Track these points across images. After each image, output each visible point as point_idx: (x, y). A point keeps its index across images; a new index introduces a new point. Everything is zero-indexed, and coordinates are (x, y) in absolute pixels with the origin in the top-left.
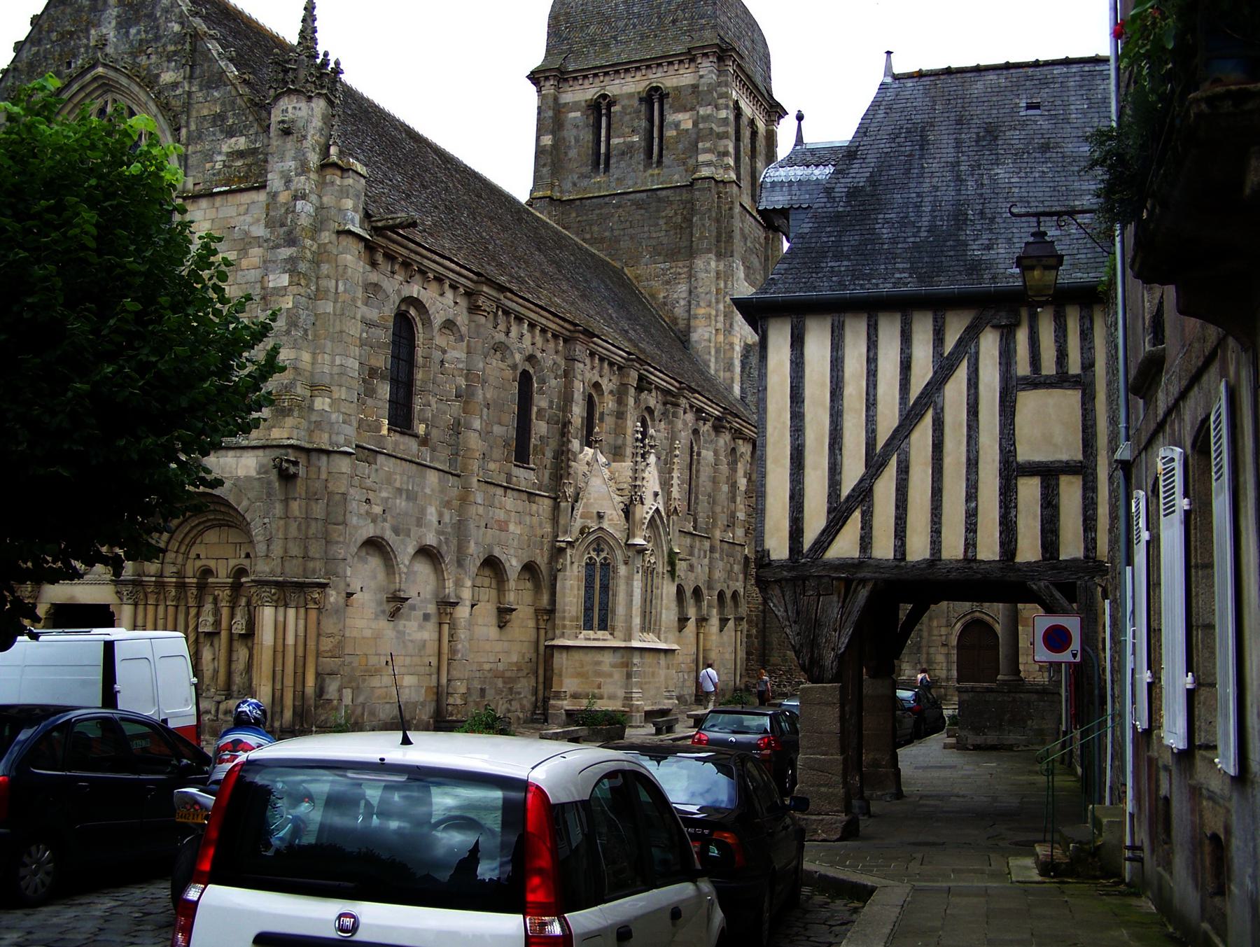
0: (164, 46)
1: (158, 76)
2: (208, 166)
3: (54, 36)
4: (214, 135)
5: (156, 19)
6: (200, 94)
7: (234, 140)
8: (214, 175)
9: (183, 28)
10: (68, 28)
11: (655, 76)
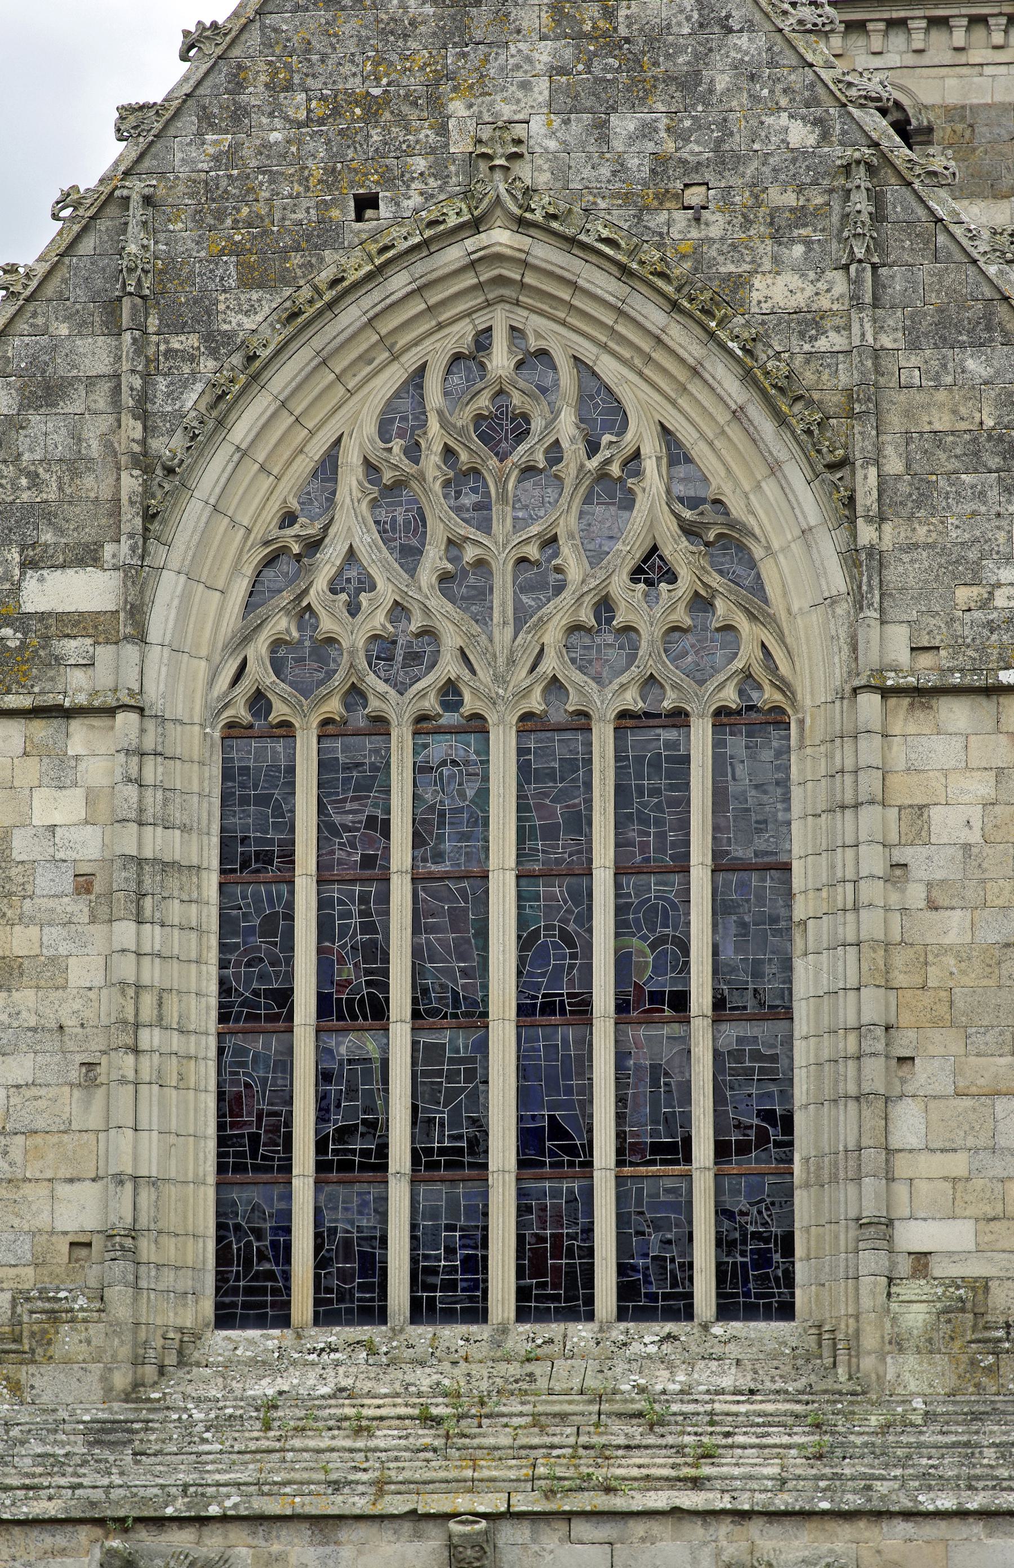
0: (757, 188)
1: (739, 283)
2: (963, 595)
3: (296, 104)
4: (982, 496)
6: (915, 360)
8: (991, 627)
9: (825, 137)
10: (355, 84)
11: (877, 62)
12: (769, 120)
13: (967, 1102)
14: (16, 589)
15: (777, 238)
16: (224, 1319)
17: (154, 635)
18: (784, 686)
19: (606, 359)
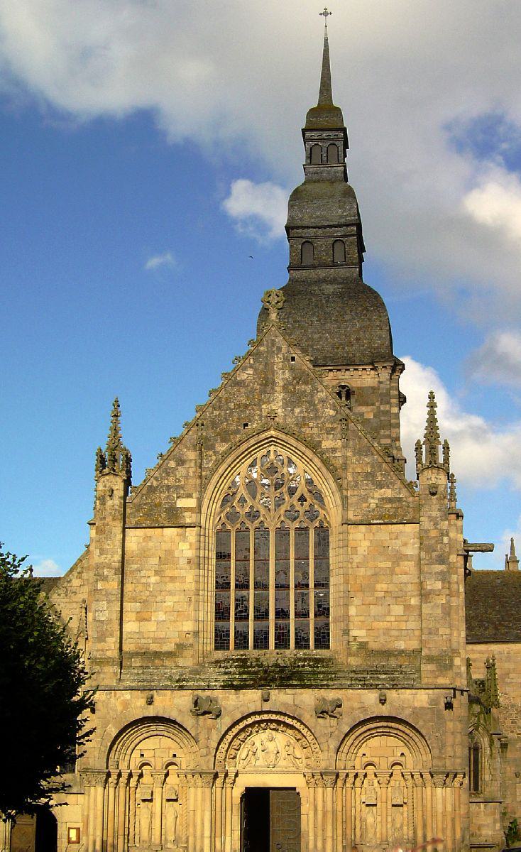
1: (320, 442)
2: (364, 505)
5: (314, 405)
7: (383, 490)
8: (369, 511)
12: (326, 410)
13: (364, 606)
14: (175, 503)
15: (327, 434)
16: (216, 648)
17: (202, 512)
18: (328, 523)
19: (293, 457)
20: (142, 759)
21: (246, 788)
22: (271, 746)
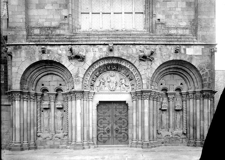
20: (43, 86)
21: (99, 101)
22: (113, 79)
